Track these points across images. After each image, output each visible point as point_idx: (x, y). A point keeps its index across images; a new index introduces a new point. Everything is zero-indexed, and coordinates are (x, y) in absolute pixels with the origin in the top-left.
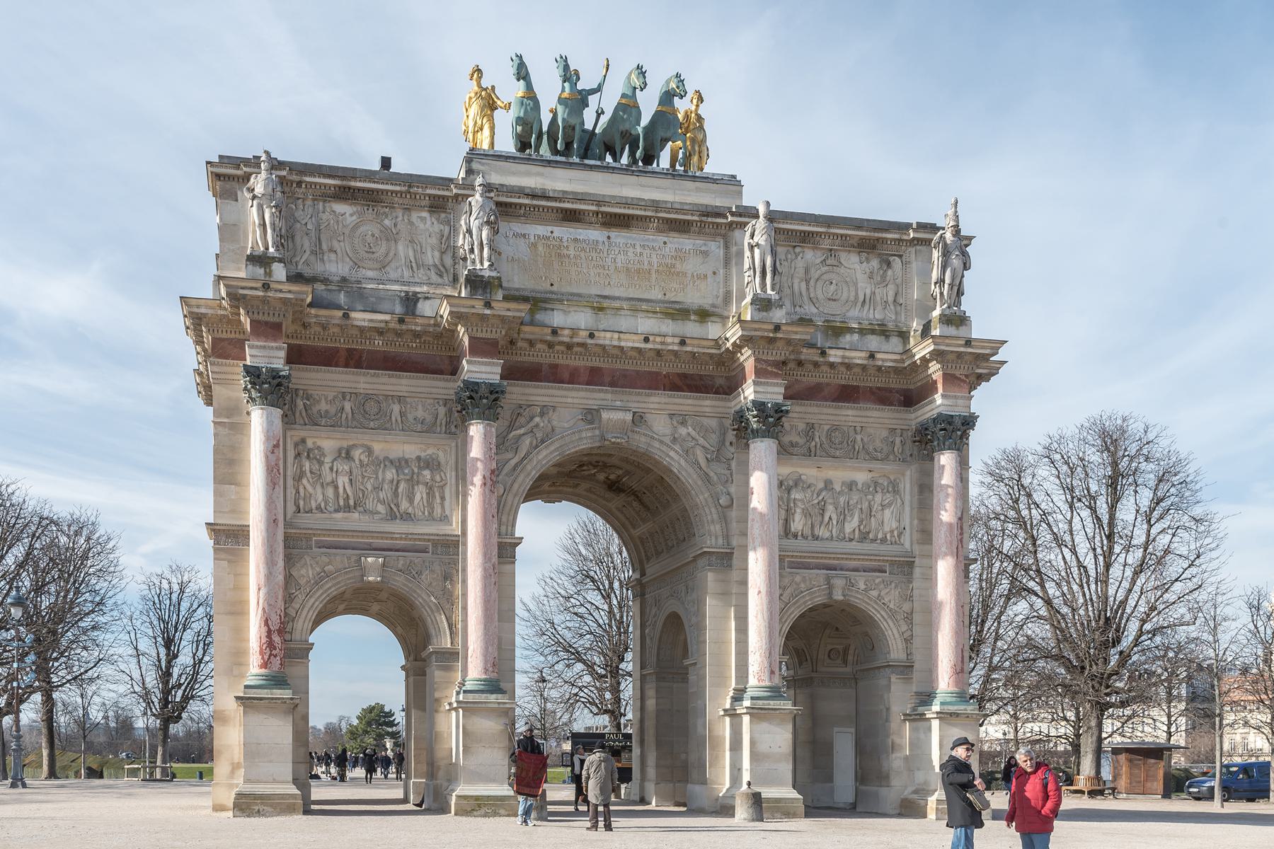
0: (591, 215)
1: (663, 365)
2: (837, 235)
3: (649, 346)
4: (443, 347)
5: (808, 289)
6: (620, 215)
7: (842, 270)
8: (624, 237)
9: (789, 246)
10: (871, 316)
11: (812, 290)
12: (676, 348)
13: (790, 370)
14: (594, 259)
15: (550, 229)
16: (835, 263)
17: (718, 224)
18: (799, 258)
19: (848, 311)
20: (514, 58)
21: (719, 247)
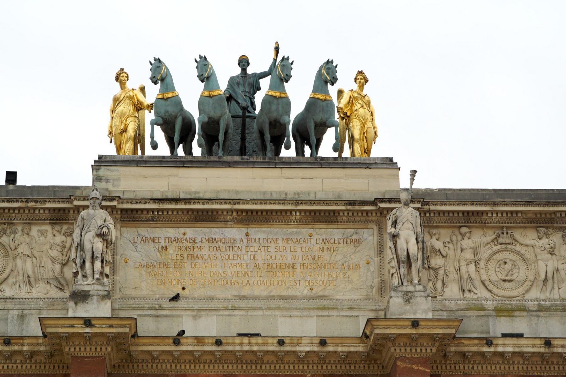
0: (225, 213)
1: (306, 367)
2: (507, 212)
3: (286, 348)
4: (56, 365)
5: (477, 271)
6: (257, 211)
7: (518, 248)
8: (264, 232)
9: (455, 227)
10: (557, 297)
11: (482, 271)
12: (316, 349)
13: (455, 363)
14: (231, 257)
15: (182, 230)
16: (510, 241)
17: (367, 212)
18: (466, 238)
19: (527, 291)
20: (153, 62)
21: (373, 234)
